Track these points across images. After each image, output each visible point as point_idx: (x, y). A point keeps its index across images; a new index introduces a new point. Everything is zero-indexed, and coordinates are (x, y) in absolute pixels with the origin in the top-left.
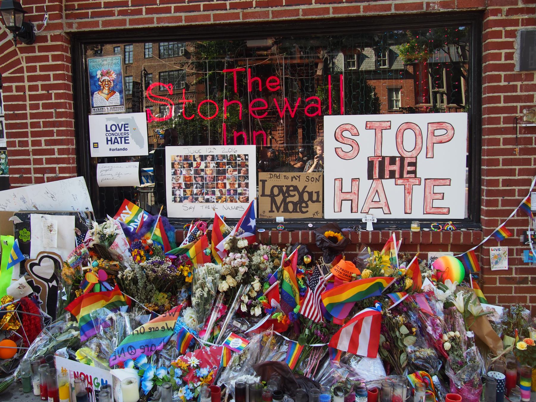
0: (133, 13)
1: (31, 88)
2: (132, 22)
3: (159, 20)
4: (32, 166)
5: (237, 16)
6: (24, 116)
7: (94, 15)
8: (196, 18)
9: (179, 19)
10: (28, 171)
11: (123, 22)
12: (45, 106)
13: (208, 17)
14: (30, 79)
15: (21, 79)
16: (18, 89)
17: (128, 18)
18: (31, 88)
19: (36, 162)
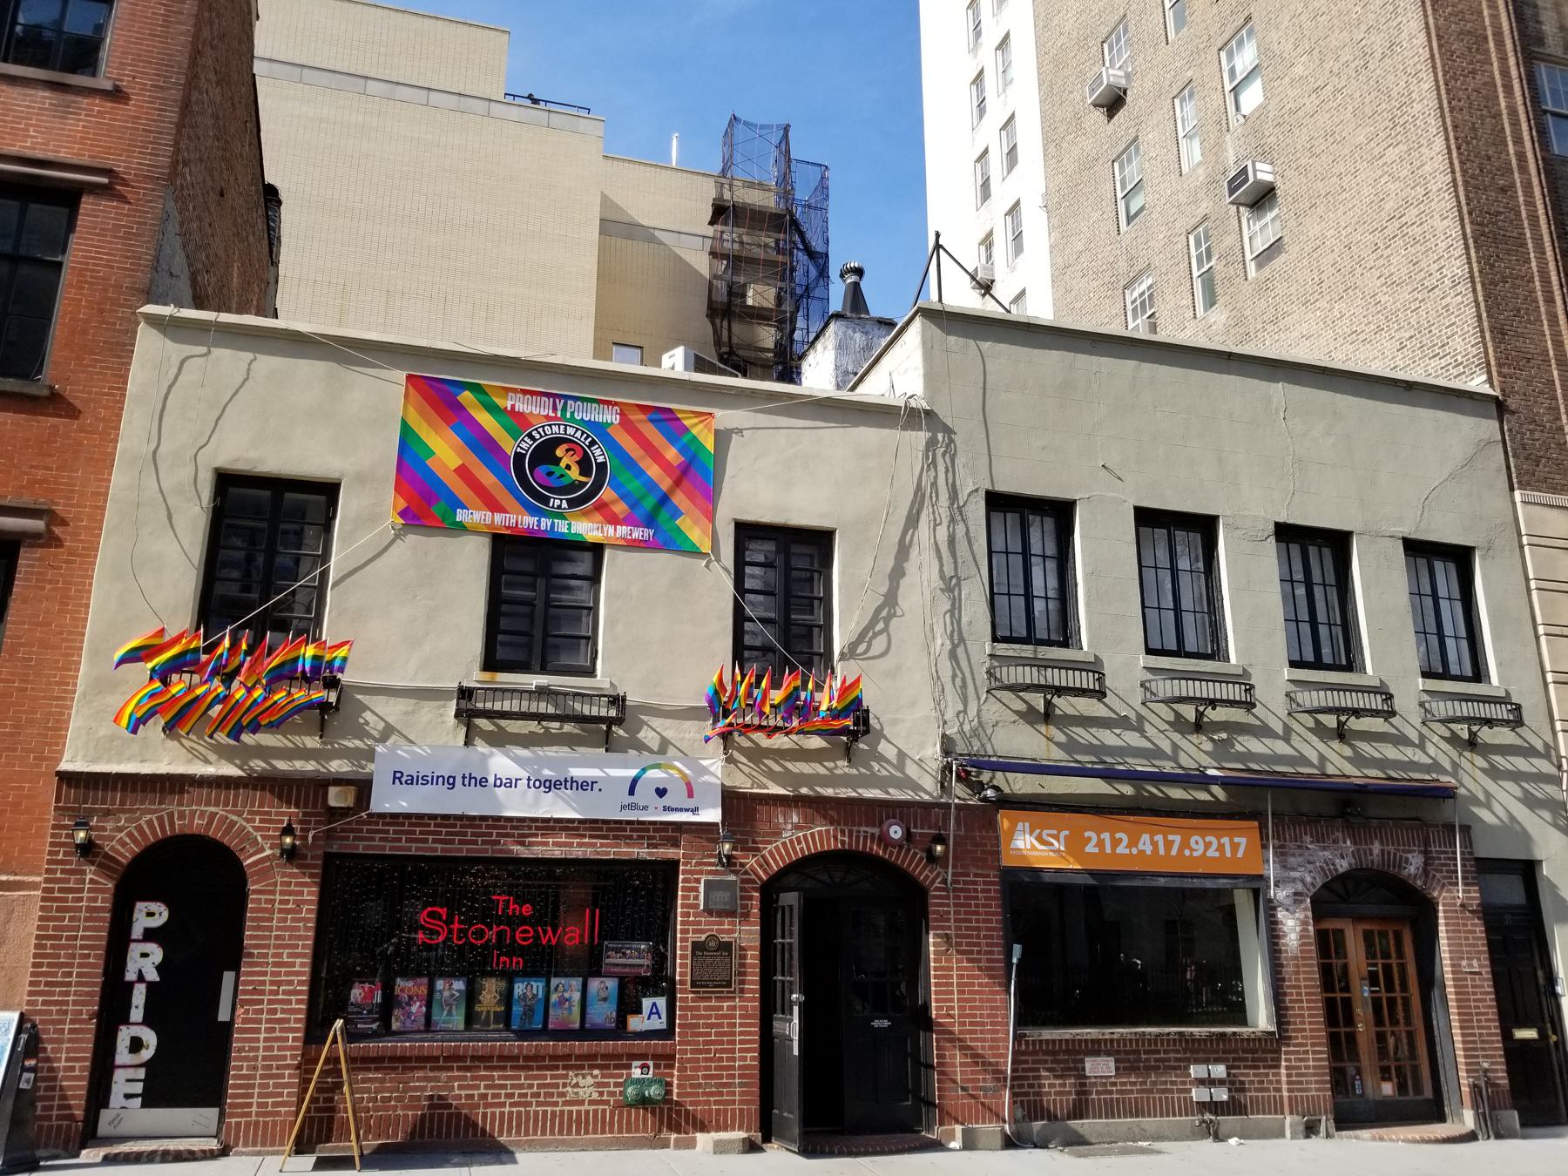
0: (393, 840)
1: (281, 902)
2: (391, 848)
3: (417, 849)
4: (268, 978)
5: (486, 851)
6: (270, 929)
7: (355, 838)
8: (450, 850)
9: (436, 850)
10: (263, 983)
11: (384, 848)
12: (293, 920)
13: (461, 850)
14: (282, 893)
15: (273, 892)
16: (267, 901)
17: (388, 845)
18: (281, 902)
19: (273, 974)
